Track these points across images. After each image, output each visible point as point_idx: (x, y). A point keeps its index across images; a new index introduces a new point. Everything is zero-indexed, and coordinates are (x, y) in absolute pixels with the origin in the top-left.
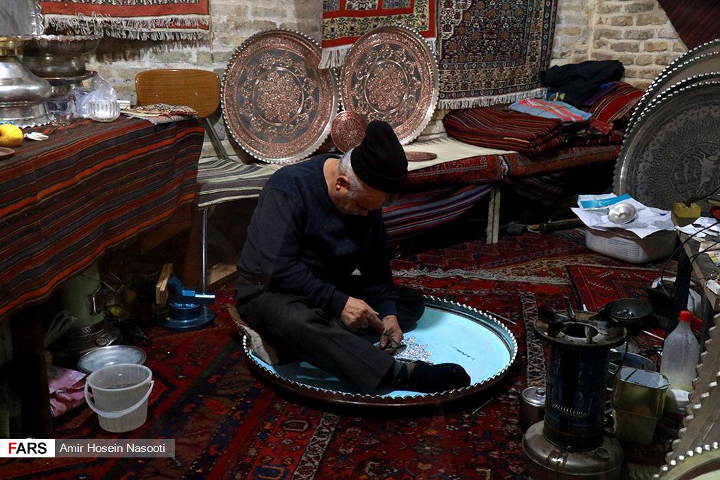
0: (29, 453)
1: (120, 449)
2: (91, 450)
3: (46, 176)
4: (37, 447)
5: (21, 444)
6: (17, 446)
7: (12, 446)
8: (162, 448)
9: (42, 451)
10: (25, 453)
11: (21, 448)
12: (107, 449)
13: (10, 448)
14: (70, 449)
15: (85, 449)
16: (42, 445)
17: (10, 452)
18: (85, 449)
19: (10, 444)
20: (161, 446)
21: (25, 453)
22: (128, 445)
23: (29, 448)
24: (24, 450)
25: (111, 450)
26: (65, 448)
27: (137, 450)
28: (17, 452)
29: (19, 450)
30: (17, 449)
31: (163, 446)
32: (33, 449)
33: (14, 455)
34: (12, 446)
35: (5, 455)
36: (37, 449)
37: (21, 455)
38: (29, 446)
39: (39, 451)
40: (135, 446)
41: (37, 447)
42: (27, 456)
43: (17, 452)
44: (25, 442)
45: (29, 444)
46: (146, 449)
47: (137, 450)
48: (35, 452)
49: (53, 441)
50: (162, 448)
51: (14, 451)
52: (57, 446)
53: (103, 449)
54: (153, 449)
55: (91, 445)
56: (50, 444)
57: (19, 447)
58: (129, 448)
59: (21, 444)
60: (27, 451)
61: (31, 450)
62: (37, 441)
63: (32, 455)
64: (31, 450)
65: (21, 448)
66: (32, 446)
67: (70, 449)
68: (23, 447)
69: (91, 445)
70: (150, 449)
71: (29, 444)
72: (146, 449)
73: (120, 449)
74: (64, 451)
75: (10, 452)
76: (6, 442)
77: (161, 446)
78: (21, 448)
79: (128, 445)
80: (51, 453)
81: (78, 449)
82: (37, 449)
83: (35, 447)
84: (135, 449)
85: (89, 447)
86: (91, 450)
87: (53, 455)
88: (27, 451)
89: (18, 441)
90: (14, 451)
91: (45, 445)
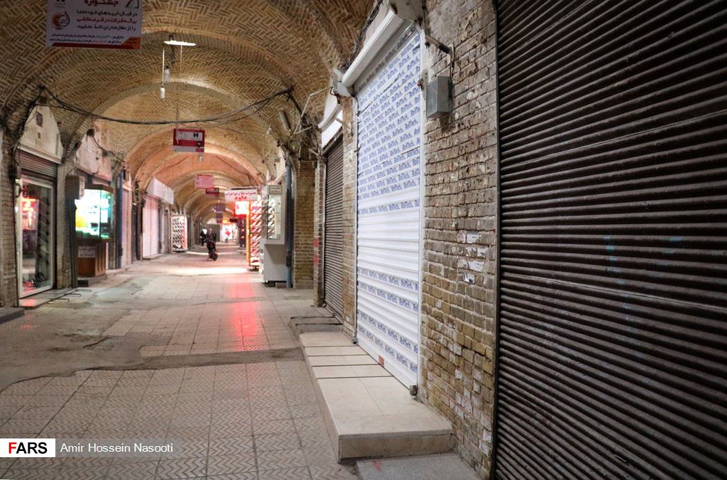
0: (29, 452)
1: (127, 448)
2: (92, 449)
5: (21, 444)
6: (17, 446)
7: (12, 445)
9: (43, 450)
10: (25, 452)
11: (21, 448)
12: (114, 448)
13: (10, 448)
14: (71, 450)
15: (86, 448)
16: (42, 445)
17: (10, 452)
19: (10, 444)
20: (168, 446)
21: (25, 452)
22: (135, 445)
23: (29, 448)
24: (24, 450)
26: (66, 448)
27: (145, 450)
28: (18, 452)
29: (19, 450)
31: (170, 445)
32: (33, 448)
33: (14, 454)
34: (12, 445)
35: (4, 453)
36: (38, 449)
37: (21, 454)
38: (29, 445)
39: (39, 451)
40: (142, 446)
42: (27, 455)
43: (18, 452)
44: (25, 441)
45: (29, 444)
47: (145, 450)
48: (36, 452)
49: (53, 440)
51: (14, 451)
53: (104, 449)
54: (161, 449)
55: (92, 445)
56: (51, 443)
57: (20, 447)
58: (137, 450)
59: (21, 444)
60: (27, 451)
61: (31, 450)
62: (38, 441)
63: (32, 454)
64: (31, 450)
65: (21, 448)
66: (32, 446)
68: (23, 447)
69: (92, 445)
70: (158, 449)
71: (29, 444)
73: (127, 448)
75: (10, 452)
76: (5, 442)
77: (168, 446)
78: (21, 448)
79: (135, 445)
80: (51, 453)
81: (80, 449)
82: (38, 449)
83: (36, 447)
84: (142, 448)
85: (90, 447)
86: (92, 449)
87: (53, 455)
88: (27, 451)
89: (18, 441)
90: (14, 451)
91: (45, 444)
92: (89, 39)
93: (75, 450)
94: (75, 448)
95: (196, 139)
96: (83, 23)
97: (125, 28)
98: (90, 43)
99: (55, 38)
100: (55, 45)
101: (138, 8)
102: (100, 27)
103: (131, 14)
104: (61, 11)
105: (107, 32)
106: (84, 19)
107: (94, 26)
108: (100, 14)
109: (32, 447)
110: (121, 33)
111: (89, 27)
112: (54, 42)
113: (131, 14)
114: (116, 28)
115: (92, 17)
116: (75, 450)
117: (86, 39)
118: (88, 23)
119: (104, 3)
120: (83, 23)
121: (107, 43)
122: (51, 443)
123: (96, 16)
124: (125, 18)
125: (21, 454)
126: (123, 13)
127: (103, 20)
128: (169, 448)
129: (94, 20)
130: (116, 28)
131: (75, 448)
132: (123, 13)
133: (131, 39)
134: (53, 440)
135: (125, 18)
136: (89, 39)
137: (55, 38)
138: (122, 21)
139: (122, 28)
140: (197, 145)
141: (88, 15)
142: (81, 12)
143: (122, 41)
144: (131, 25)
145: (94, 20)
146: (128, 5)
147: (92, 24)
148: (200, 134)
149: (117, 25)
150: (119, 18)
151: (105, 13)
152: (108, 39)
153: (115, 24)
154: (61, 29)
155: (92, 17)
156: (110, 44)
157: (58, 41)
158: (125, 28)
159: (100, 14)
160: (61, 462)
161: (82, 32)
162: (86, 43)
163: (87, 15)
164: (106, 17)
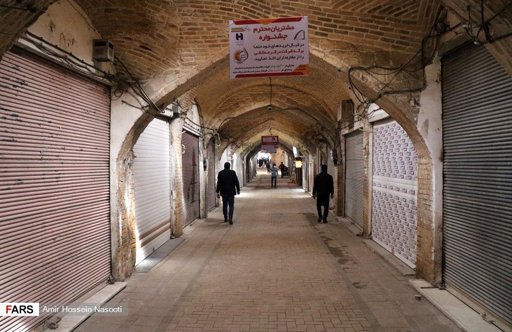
3: (228, 93)
92: (265, 69)
95: (274, 141)
96: (259, 57)
97: (295, 57)
98: (266, 72)
99: (237, 70)
100: (238, 76)
101: (304, 39)
102: (274, 58)
103: (299, 45)
104: (241, 48)
105: (280, 62)
106: (260, 53)
107: (268, 58)
108: (273, 47)
110: (291, 61)
111: (264, 59)
112: (237, 74)
113: (299, 45)
114: (287, 58)
115: (267, 50)
117: (262, 69)
118: (264, 56)
119: (276, 38)
120: (259, 57)
121: (280, 72)
123: (269, 50)
124: (293, 48)
126: (292, 45)
127: (275, 52)
129: (269, 53)
130: (287, 58)
132: (292, 45)
133: (300, 66)
135: (293, 48)
136: (265, 69)
137: (237, 70)
138: (292, 51)
139: (293, 58)
140: (274, 144)
141: (263, 49)
142: (257, 47)
143: (293, 69)
144: (299, 54)
145: (269, 53)
146: (295, 38)
147: (267, 56)
148: (276, 138)
149: (286, 55)
150: (289, 49)
151: (277, 46)
152: (281, 68)
153: (286, 55)
154: (241, 63)
155: (267, 50)
156: (283, 72)
157: (240, 74)
158: (295, 57)
159: (273, 47)
161: (262, 63)
162: (263, 73)
163: (262, 49)
164: (278, 49)
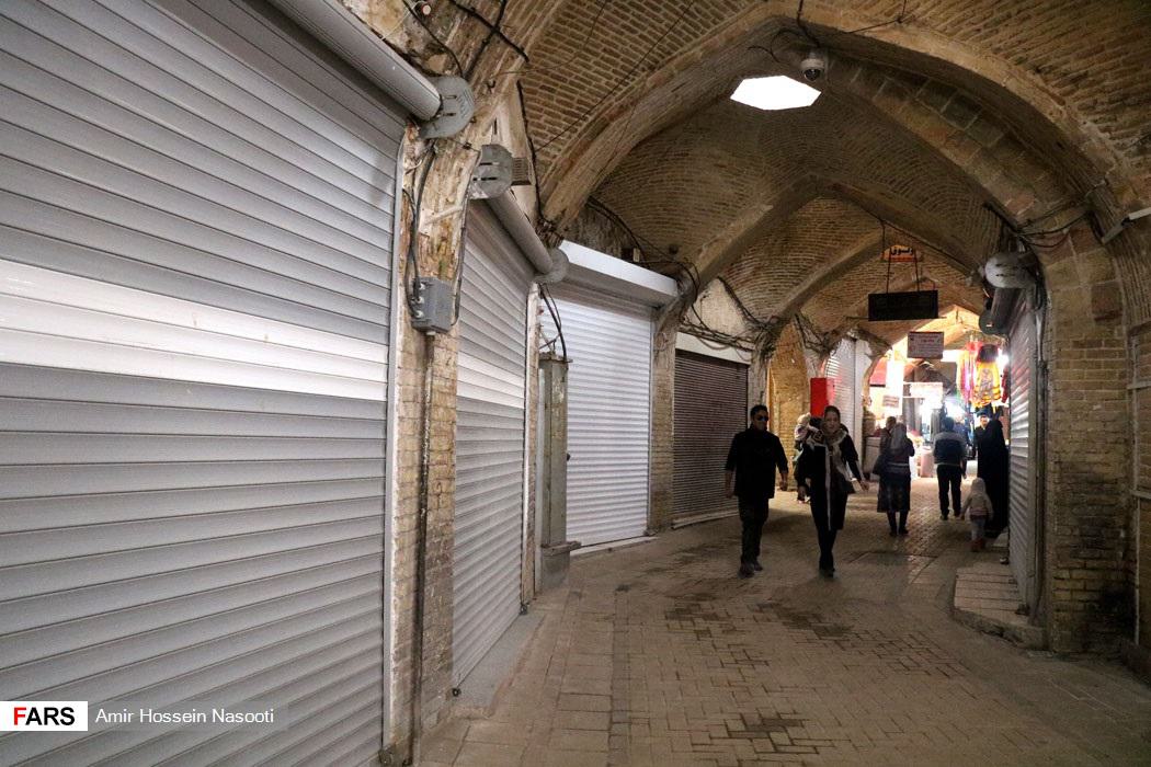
0: (46, 723)
1: (202, 718)
2: (146, 718)
4: (60, 714)
5: (34, 710)
6: (27, 713)
7: (20, 712)
8: (269, 717)
9: (68, 720)
10: (40, 723)
11: (34, 716)
13: (17, 716)
14: (112, 717)
16: (67, 712)
17: (16, 723)
18: (136, 719)
19: (16, 710)
20: (267, 714)
21: (40, 723)
22: (215, 711)
23: (46, 716)
24: (38, 719)
25: (187, 719)
27: (230, 719)
28: (28, 723)
29: (30, 719)
30: (27, 717)
31: (270, 712)
32: (53, 717)
33: (22, 726)
34: (20, 712)
35: (9, 726)
36: (59, 717)
37: (34, 726)
38: (46, 713)
39: (63, 721)
41: (60, 714)
42: (43, 728)
43: (28, 723)
44: (40, 706)
45: (46, 709)
46: (243, 717)
47: (230, 719)
48: (57, 723)
49: (84, 705)
50: (269, 717)
51: (22, 721)
52: (92, 713)
54: (255, 718)
56: (81, 709)
57: (31, 714)
58: (216, 716)
59: (34, 710)
61: (49, 719)
62: (60, 705)
63: (51, 726)
64: (49, 719)
65: (33, 716)
66: (51, 713)
67: (112, 717)
68: (37, 715)
71: (46, 709)
72: (243, 717)
73: (202, 718)
74: (102, 720)
75: (16, 723)
78: (34, 716)
79: (215, 711)
80: (81, 724)
82: (59, 717)
83: (56, 714)
86: (146, 718)
87: (84, 727)
89: (29, 705)
90: (22, 721)
91: (72, 711)
93: (118, 719)
94: (118, 717)
109: (50, 715)
116: (118, 719)
122: (81, 709)
125: (34, 726)
128: (267, 716)
131: (118, 717)
134: (84, 705)
160: (97, 736)
